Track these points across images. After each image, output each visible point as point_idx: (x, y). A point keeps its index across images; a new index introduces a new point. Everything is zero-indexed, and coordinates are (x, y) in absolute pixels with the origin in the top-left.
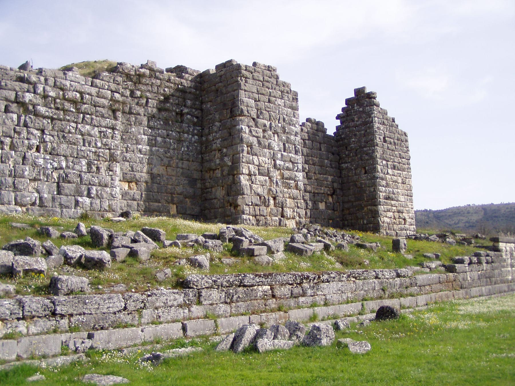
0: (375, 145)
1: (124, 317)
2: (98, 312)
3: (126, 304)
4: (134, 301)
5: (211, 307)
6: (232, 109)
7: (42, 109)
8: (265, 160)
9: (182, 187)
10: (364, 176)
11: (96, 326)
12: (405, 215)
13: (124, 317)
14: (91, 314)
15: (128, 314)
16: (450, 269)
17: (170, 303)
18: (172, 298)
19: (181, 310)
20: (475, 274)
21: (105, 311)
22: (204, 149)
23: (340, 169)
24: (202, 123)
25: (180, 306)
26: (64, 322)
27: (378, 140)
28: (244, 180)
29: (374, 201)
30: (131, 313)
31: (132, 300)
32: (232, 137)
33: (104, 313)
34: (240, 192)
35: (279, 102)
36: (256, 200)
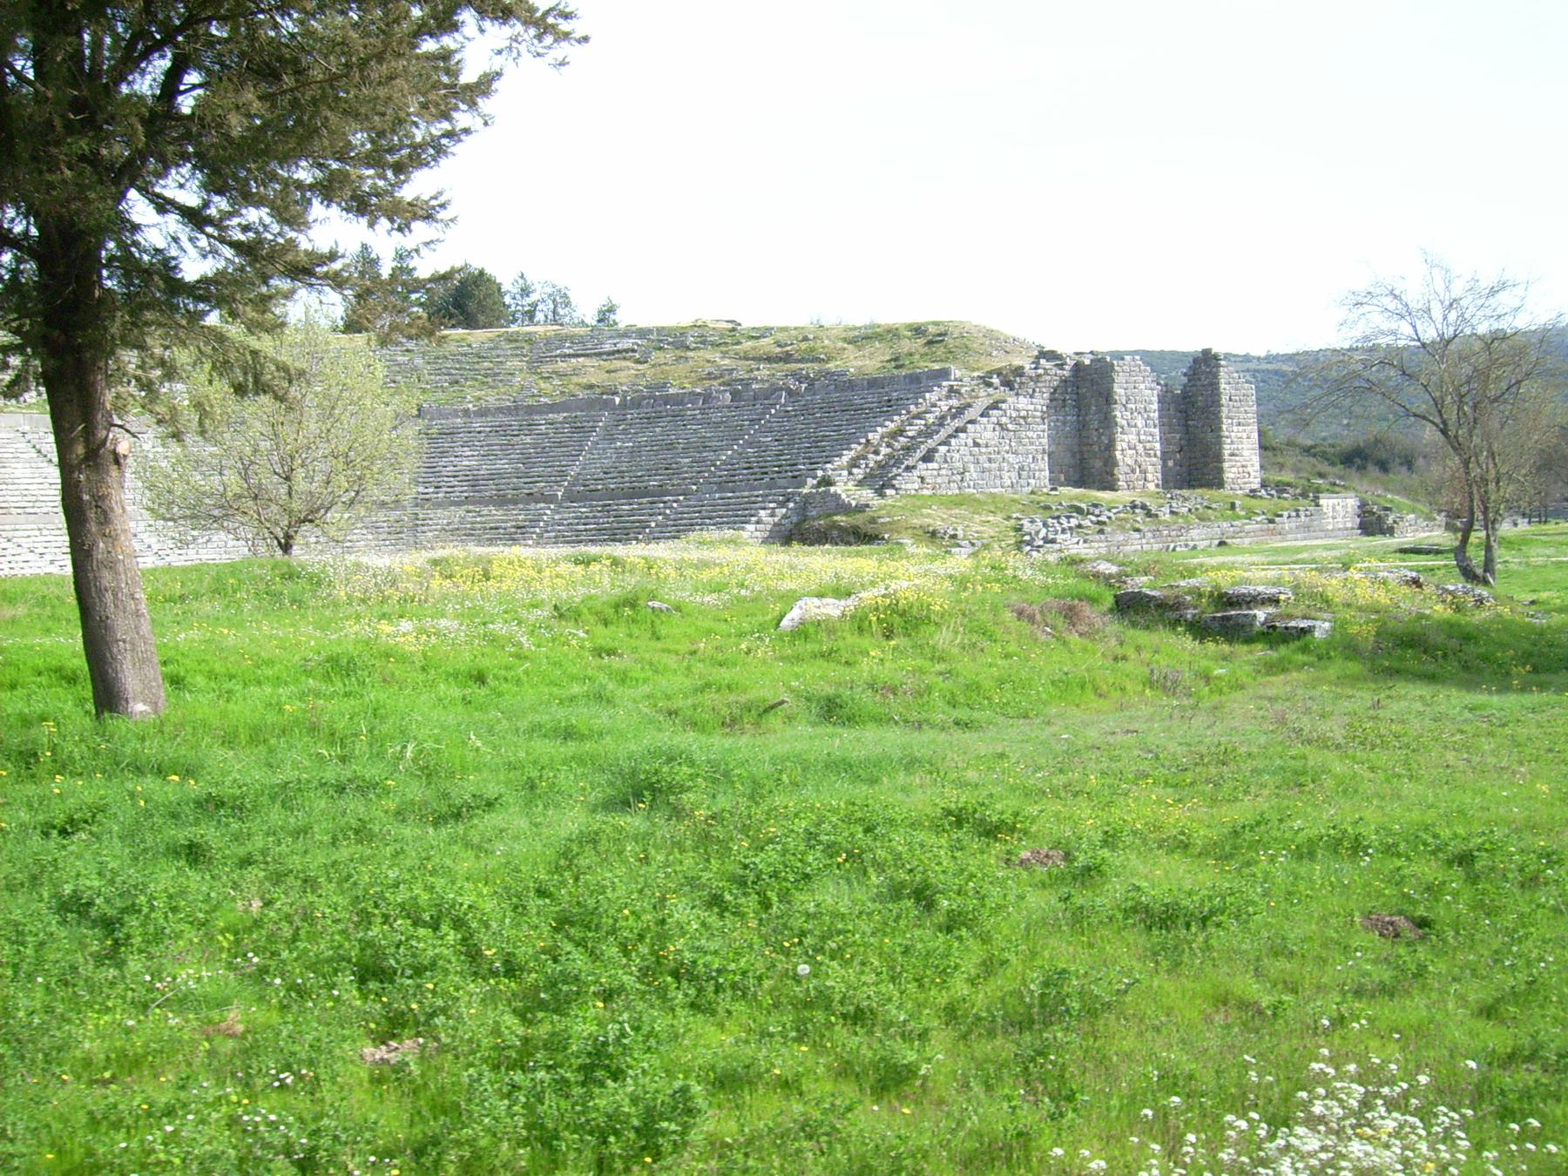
0: (1220, 406)
6: (1108, 398)
7: (1010, 426)
8: (1133, 438)
9: (1068, 460)
10: (1210, 435)
12: (1249, 469)
16: (1271, 521)
20: (1293, 525)
22: (1082, 426)
23: (1187, 426)
24: (1080, 406)
27: (1224, 400)
28: (1118, 454)
29: (1219, 458)
32: (1108, 422)
34: (1115, 464)
35: (1142, 386)
36: (1127, 470)
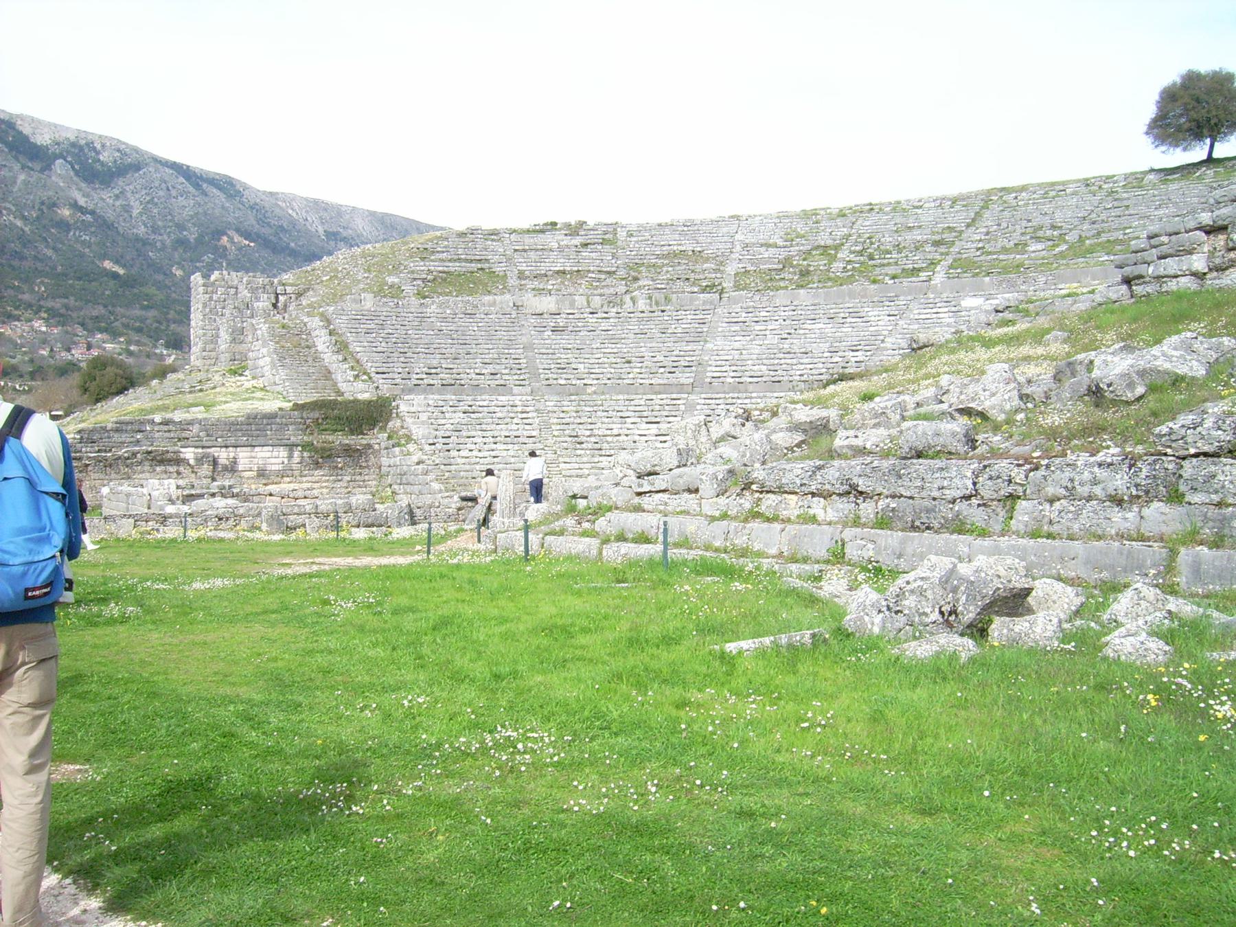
1: (974, 513)
2: (924, 494)
3: (974, 484)
4: (991, 478)
5: (1213, 512)
11: (917, 523)
13: (974, 513)
14: (911, 498)
15: (979, 505)
17: (1084, 491)
18: (1086, 475)
19: (1116, 515)
21: (936, 494)
25: (1118, 501)
26: (868, 509)
30: (984, 505)
31: (986, 476)
33: (934, 499)
